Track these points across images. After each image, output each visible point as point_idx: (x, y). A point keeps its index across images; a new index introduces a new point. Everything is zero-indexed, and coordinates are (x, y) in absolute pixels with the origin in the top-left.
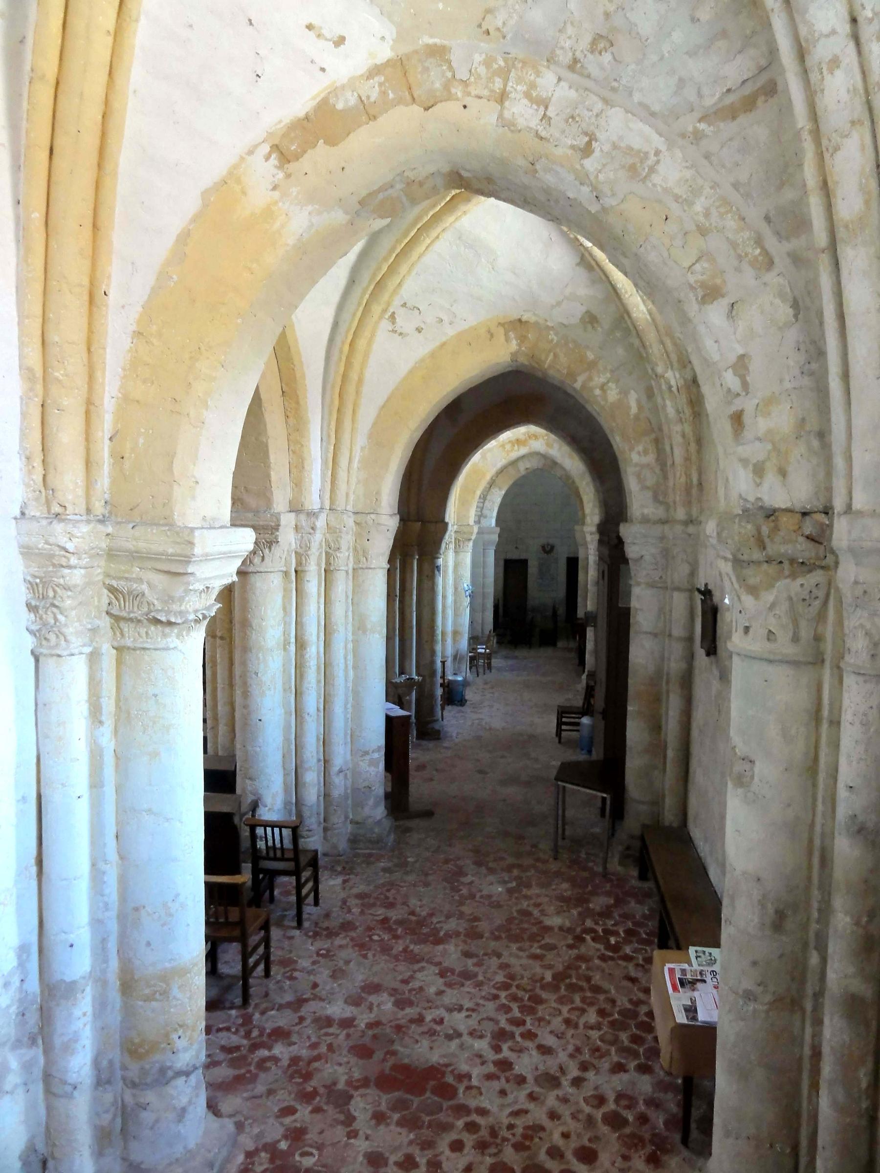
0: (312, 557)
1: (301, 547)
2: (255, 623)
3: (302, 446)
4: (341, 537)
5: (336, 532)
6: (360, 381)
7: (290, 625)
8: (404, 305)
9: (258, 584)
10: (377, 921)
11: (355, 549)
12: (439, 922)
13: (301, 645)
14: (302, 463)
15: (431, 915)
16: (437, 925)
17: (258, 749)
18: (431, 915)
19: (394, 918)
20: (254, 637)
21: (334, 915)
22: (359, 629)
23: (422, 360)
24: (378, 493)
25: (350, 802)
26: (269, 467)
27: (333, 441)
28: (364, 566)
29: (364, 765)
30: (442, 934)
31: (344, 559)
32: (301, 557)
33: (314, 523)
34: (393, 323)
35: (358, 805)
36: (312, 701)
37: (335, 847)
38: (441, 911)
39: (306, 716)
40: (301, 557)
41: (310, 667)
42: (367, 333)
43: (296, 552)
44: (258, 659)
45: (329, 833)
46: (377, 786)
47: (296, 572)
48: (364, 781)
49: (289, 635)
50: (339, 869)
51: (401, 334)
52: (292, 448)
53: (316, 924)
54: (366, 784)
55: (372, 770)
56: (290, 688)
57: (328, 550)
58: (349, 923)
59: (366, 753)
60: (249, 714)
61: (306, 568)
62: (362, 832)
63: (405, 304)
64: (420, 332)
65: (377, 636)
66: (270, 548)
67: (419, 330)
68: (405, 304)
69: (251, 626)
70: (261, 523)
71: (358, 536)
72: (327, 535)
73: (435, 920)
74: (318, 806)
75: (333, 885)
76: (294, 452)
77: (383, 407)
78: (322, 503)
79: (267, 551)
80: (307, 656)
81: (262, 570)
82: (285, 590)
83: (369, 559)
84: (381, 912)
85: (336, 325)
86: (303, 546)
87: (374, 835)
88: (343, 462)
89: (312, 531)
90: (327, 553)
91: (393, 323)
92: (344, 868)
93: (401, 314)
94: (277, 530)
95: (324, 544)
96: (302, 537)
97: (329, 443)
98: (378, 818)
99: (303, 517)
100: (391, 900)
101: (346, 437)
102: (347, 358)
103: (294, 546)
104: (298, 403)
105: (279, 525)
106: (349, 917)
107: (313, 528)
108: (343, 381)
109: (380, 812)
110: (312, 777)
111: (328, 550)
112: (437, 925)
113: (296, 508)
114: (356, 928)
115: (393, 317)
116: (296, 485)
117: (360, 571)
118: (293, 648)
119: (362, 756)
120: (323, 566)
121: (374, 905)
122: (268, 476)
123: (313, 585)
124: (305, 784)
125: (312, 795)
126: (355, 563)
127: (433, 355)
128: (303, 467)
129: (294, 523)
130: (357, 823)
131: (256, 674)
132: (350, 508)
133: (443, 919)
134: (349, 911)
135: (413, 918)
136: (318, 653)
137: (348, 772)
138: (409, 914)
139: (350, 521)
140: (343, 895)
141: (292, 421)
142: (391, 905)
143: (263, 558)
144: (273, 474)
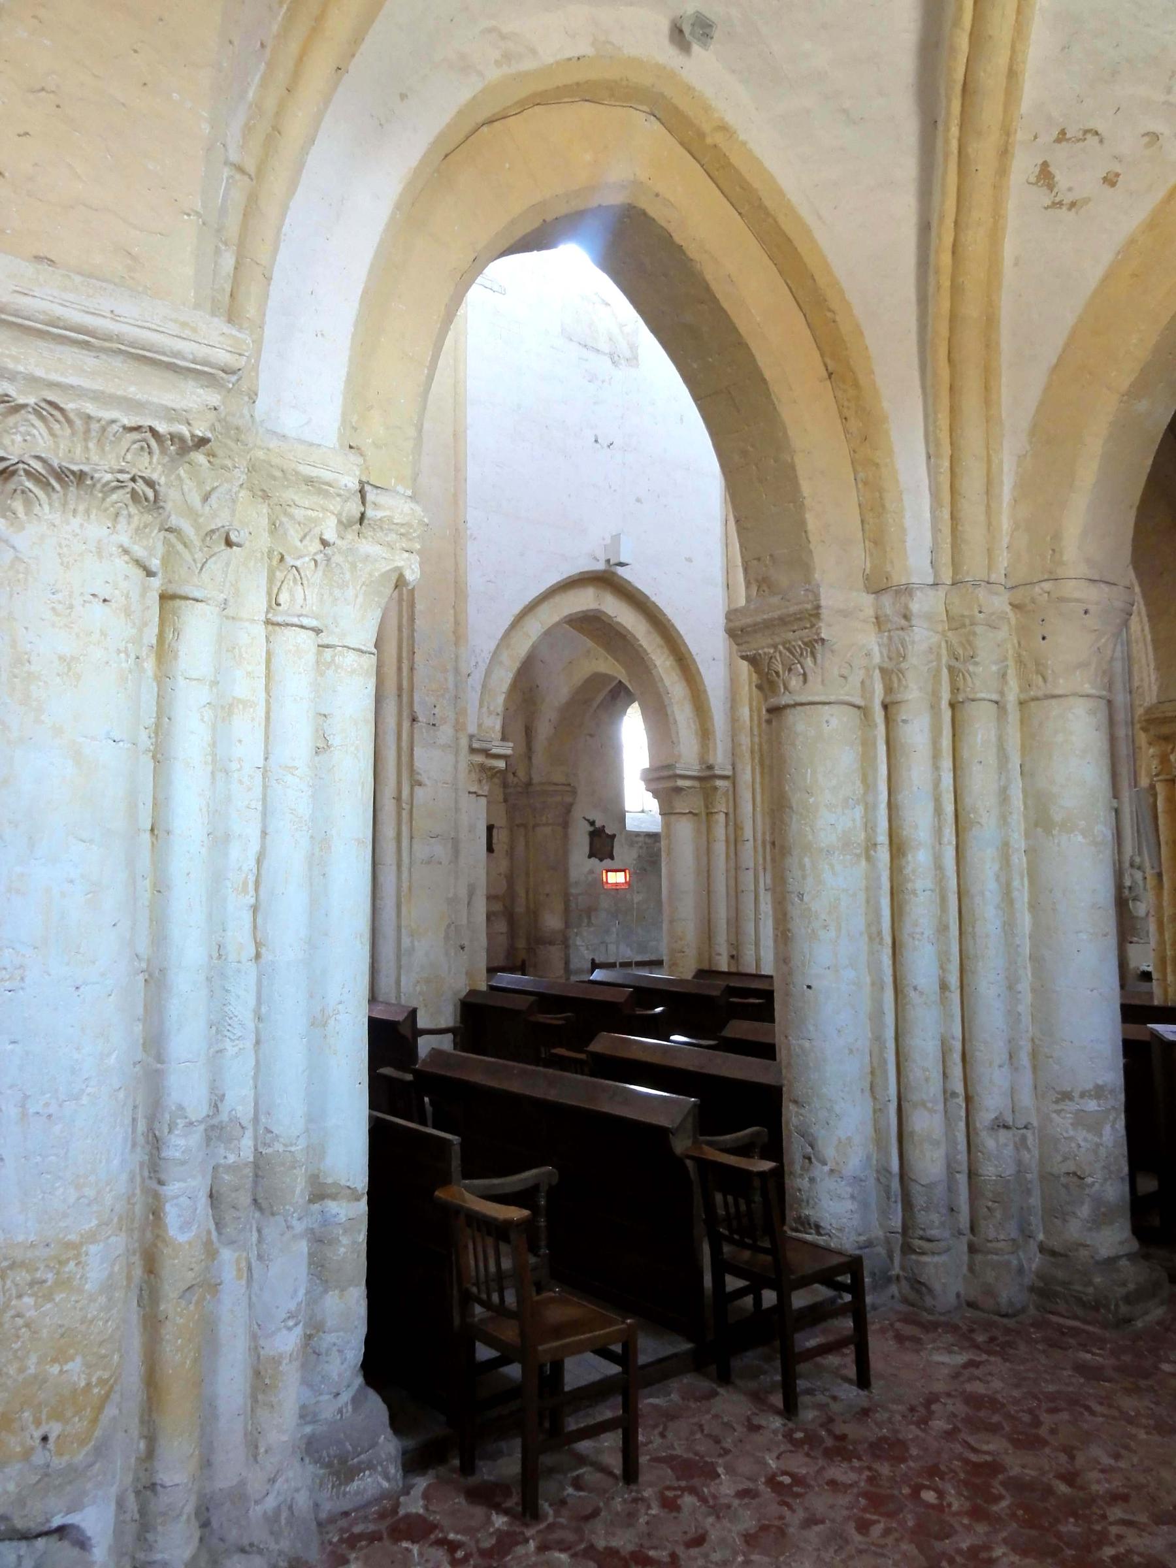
0: (910, 675)
1: (890, 659)
2: (795, 798)
3: (877, 465)
4: (975, 634)
5: (963, 626)
6: (990, 321)
7: (875, 807)
8: (1062, 137)
9: (800, 727)
10: (967, 1462)
11: (1020, 661)
12: (1128, 1523)
13: (897, 848)
14: (881, 498)
15: (1117, 1498)
16: (1114, 1530)
17: (807, 1044)
18: (1117, 1498)
19: (1013, 1473)
20: (794, 826)
21: (881, 1416)
22: (1036, 825)
23: (1132, 241)
24: (1057, 537)
25: (1035, 1201)
26: (802, 505)
27: (946, 450)
28: (1040, 694)
29: (1062, 1124)
30: (1108, 1552)
31: (983, 677)
32: (891, 675)
33: (906, 607)
34: (1051, 187)
35: (1056, 1213)
36: (925, 965)
37: (989, 1292)
38: (1154, 1500)
39: (912, 994)
40: (891, 675)
41: (914, 892)
42: (979, 214)
43: (883, 670)
44: (802, 867)
45: (979, 1258)
46: (1099, 1175)
47: (885, 707)
48: (1065, 1159)
49: (874, 829)
50: (981, 1338)
51: (1073, 205)
52: (861, 475)
53: (831, 1420)
54: (1071, 1166)
55: (1083, 1138)
56: (880, 933)
57: (953, 663)
58: (902, 1444)
59: (1066, 1096)
60: (790, 973)
61: (899, 697)
62: (1060, 1274)
63: (1063, 132)
64: (1113, 184)
65: (1080, 838)
66: (813, 655)
67: (1110, 181)
68: (1063, 132)
69: (791, 808)
70: (792, 609)
71: (1023, 631)
72: (950, 634)
73: (1117, 1512)
74: (951, 1188)
75: (938, 1363)
76: (866, 483)
77: (1056, 366)
78: (936, 574)
79: (809, 661)
80: (908, 871)
81: (803, 699)
82: (864, 743)
83: (1050, 679)
84: (992, 1446)
85: (925, 228)
86: (894, 655)
87: (1091, 1290)
88: (972, 485)
89: (903, 622)
90: (951, 669)
91: (1051, 187)
92: (992, 1339)
93: (1060, 158)
94: (817, 616)
95: (944, 652)
96: (890, 638)
97: (939, 456)
98: (1105, 1252)
99: (887, 600)
100: (1043, 1431)
101: (973, 435)
102: (953, 280)
103: (877, 659)
104: (856, 385)
105: (818, 607)
106: (910, 1432)
107: (906, 617)
108: (952, 330)
109: (1113, 1239)
110: (927, 1123)
111: (953, 663)
112: (1114, 1530)
113: (878, 585)
114: (903, 1460)
115: (1045, 175)
116: (876, 543)
117: (1032, 704)
118: (883, 855)
119: (1057, 1102)
120: (946, 696)
121: (994, 1429)
122: (802, 523)
123: (917, 732)
124: (912, 1133)
125: (931, 1164)
126: (1022, 690)
127: (1152, 224)
128: (883, 506)
129: (870, 612)
130: (1053, 1253)
131: (801, 896)
132: (998, 576)
133: (1143, 1518)
134: (923, 1422)
135: (1062, 1488)
136: (939, 867)
137: (1029, 1133)
138: (1062, 1477)
139: (999, 603)
140: (939, 1387)
141: (854, 425)
142: (1029, 1442)
143: (805, 675)
144: (809, 517)
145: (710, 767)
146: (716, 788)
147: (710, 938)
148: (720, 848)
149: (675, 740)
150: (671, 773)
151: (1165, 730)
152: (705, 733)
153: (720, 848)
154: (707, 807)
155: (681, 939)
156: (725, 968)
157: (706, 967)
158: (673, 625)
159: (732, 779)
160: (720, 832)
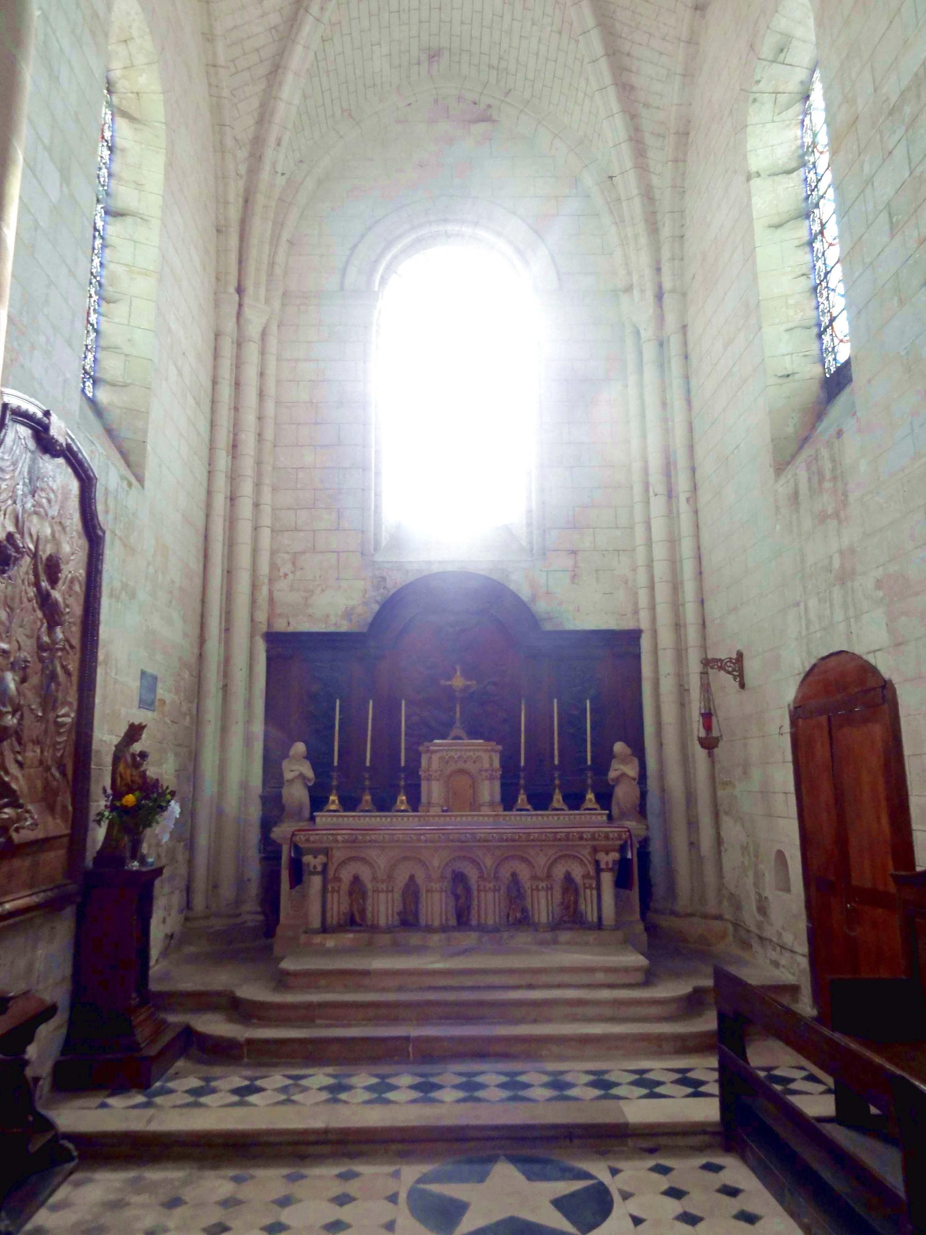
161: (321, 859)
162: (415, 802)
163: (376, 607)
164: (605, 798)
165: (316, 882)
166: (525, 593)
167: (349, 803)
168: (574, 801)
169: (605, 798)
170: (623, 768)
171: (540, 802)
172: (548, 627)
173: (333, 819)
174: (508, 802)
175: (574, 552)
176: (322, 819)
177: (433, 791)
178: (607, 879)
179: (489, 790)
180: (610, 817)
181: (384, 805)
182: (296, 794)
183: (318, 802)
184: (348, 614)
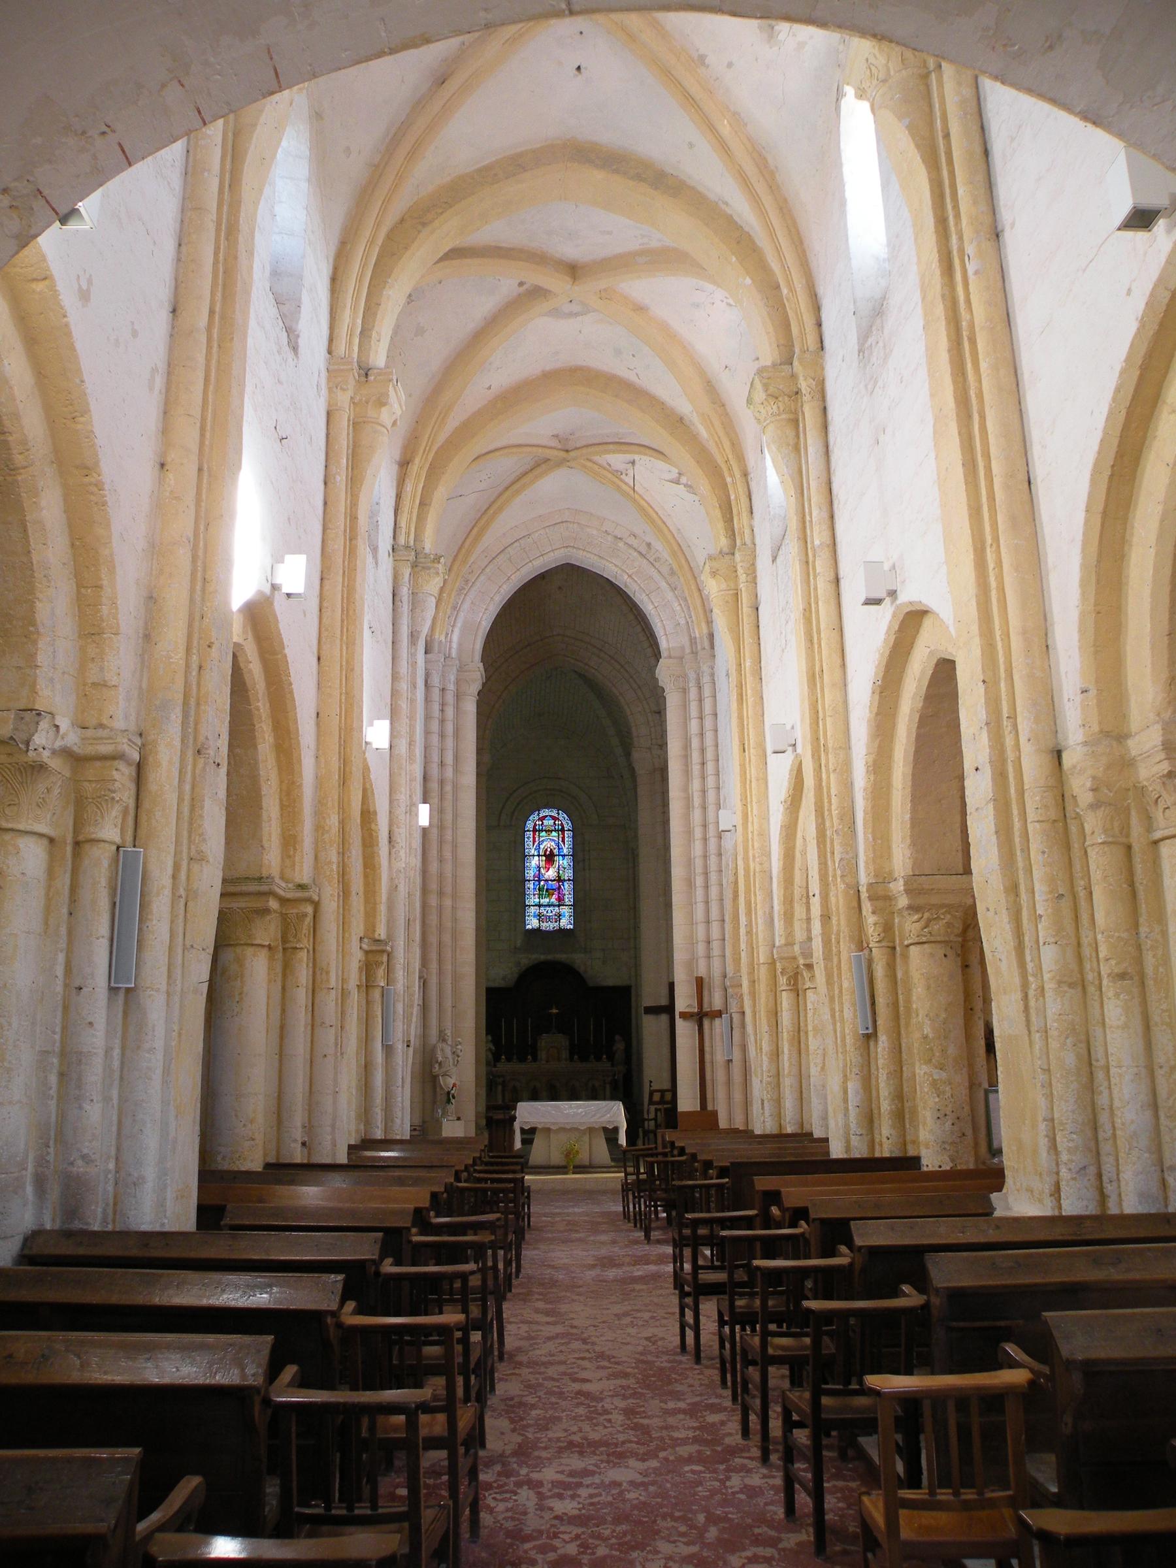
145: (301, 887)
146: (305, 915)
147: (279, 1122)
148: (301, 996)
149: (266, 845)
150: (264, 888)
151: (921, 901)
152: (290, 842)
153: (301, 996)
154: (284, 940)
155: (251, 1122)
156: (298, 1161)
157: (273, 1161)
158: (291, 692)
159: (316, 905)
160: (303, 975)
161: (501, 1080)
162: (535, 1059)
163: (516, 976)
164: (611, 1058)
165: (500, 1088)
166: (581, 970)
167: (509, 1060)
168: (598, 1059)
169: (611, 1058)
170: (619, 1046)
171: (584, 1059)
172: (591, 985)
173: (503, 1066)
174: (571, 1059)
175: (603, 950)
176: (498, 1065)
177: (542, 1055)
178: (608, 1086)
179: (565, 1054)
180: (613, 1065)
181: (522, 1059)
182: (490, 1056)
183: (497, 1058)
184: (504, 979)
